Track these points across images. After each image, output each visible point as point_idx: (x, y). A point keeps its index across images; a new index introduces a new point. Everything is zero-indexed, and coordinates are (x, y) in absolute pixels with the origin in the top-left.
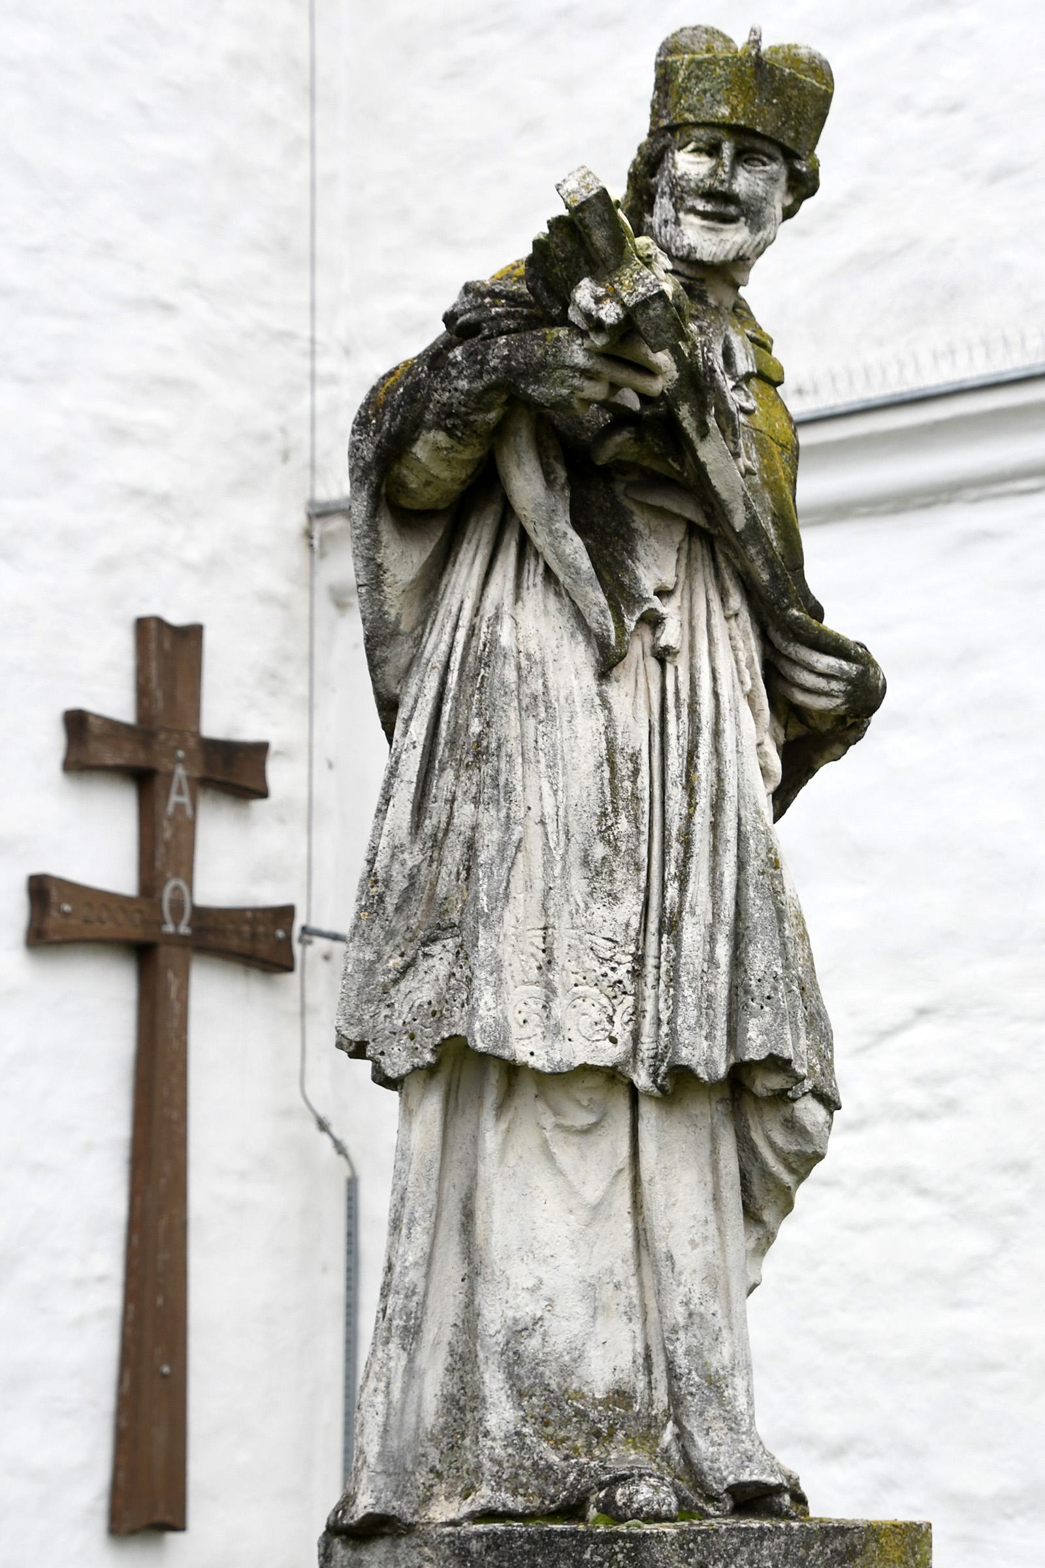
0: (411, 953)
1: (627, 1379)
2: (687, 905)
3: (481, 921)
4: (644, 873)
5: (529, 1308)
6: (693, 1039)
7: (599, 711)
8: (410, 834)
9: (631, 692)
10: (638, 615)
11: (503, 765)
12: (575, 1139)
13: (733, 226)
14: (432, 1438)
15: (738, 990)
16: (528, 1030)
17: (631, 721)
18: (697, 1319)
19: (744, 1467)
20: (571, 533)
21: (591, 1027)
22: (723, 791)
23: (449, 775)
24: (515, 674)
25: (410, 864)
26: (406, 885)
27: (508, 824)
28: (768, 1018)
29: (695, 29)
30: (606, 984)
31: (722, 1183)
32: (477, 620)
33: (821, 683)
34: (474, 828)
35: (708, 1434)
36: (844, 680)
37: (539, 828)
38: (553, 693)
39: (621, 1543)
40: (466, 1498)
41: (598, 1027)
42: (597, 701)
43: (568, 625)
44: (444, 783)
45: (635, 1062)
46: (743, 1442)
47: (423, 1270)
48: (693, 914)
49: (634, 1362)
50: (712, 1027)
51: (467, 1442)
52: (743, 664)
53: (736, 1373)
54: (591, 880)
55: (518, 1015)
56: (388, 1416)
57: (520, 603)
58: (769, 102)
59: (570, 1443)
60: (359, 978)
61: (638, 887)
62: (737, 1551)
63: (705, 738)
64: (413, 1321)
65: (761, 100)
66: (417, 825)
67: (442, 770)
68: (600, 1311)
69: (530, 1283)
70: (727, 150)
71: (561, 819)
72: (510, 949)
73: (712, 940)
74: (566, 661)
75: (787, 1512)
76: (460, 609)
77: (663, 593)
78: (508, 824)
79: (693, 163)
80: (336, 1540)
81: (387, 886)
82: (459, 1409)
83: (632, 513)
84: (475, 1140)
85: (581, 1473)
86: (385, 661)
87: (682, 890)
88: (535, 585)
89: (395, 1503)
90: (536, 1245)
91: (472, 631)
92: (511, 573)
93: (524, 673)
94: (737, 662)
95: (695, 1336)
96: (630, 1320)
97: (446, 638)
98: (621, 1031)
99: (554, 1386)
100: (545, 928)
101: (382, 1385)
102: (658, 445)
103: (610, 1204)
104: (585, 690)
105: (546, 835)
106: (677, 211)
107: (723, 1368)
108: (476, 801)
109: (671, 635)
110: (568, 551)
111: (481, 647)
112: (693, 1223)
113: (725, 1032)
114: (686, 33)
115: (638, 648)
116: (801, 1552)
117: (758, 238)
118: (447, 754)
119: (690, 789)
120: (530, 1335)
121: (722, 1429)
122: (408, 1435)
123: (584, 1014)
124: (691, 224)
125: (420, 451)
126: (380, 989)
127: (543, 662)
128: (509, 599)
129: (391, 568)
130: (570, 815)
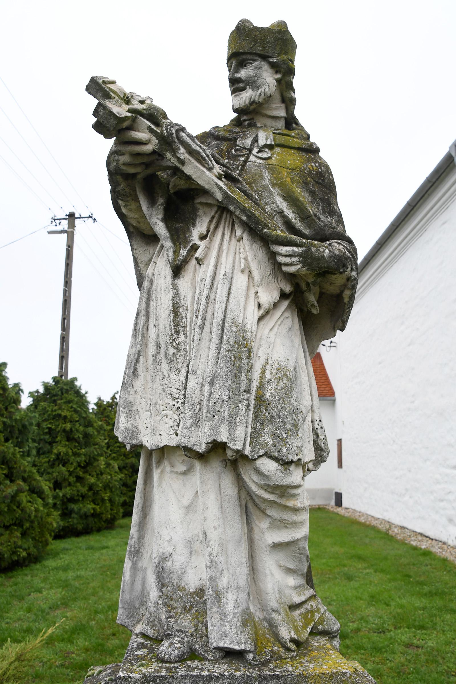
5: (168, 549)
6: (188, 434)
7: (171, 291)
10: (188, 248)
12: (181, 477)
19: (221, 639)
21: (169, 428)
30: (175, 409)
33: (287, 260)
36: (297, 256)
42: (171, 287)
46: (226, 626)
53: (229, 591)
58: (244, 40)
65: (241, 40)
68: (194, 553)
72: (139, 397)
83: (199, 209)
89: (126, 621)
99: (175, 584)
103: (196, 506)
110: (157, 229)
112: (214, 518)
121: (217, 618)
123: (166, 423)
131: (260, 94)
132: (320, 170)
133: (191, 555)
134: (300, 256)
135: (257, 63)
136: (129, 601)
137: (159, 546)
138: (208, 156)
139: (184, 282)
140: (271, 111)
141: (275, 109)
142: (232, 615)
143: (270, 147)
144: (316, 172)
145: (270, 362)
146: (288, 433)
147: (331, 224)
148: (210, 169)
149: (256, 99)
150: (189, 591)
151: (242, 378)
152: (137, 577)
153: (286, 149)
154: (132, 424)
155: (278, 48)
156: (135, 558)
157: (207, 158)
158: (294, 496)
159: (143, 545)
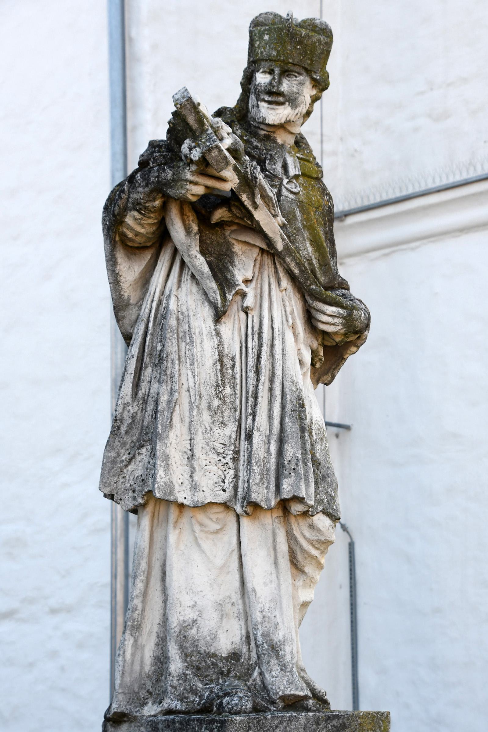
0: (133, 453)
1: (238, 648)
2: (255, 427)
3: (158, 437)
4: (238, 413)
5: (190, 615)
6: (258, 490)
7: (214, 337)
8: (132, 397)
9: (231, 328)
10: (234, 292)
11: (169, 365)
12: (211, 536)
13: (283, 107)
14: (149, 676)
15: (280, 466)
16: (183, 488)
17: (231, 342)
18: (267, 619)
20: (199, 256)
21: (213, 485)
22: (274, 373)
23: (149, 370)
24: (175, 322)
25: (132, 412)
26: (130, 421)
27: (172, 392)
28: (293, 479)
29: (266, 14)
30: (221, 464)
31: (278, 555)
32: (162, 297)
33: (330, 319)
34: (158, 394)
35: (271, 672)
36: (341, 318)
37: (187, 393)
38: (192, 330)
39: (216, 724)
40: (160, 704)
41: (217, 485)
42: (214, 333)
43: (201, 298)
44: (148, 372)
45: (236, 500)
47: (141, 599)
48: (259, 431)
49: (241, 639)
50: (269, 483)
51: (163, 678)
52: (288, 313)
53: (286, 644)
54: (212, 416)
55: (179, 481)
56: (124, 666)
57: (180, 289)
59: (209, 678)
60: (109, 465)
61: (235, 419)
62: (277, 727)
63: (265, 349)
64: (136, 623)
66: (135, 394)
67: (146, 367)
68: (225, 616)
69: (191, 603)
70: (277, 71)
71: (197, 389)
72: (174, 450)
73: (269, 443)
74: (199, 315)
75: (311, 708)
76: (155, 292)
77: (247, 282)
78: (172, 392)
79: (262, 78)
80: (108, 724)
81: (121, 422)
82: (161, 663)
84: (166, 538)
85: (211, 692)
86: (123, 317)
87: (254, 420)
88: (187, 280)
90: (193, 586)
91: (160, 302)
92: (176, 276)
93: (180, 321)
94: (286, 312)
95: (266, 627)
96: (239, 620)
97: (148, 306)
98: (228, 486)
100: (191, 440)
101: (121, 652)
102: (239, 213)
103: (229, 566)
104: (208, 328)
105: (190, 396)
106: (257, 101)
107: (280, 641)
108: (159, 382)
109: (249, 301)
110: (197, 264)
111: (163, 310)
113: (274, 485)
114: (262, 16)
115: (234, 308)
116: (314, 726)
118: (148, 360)
119: (258, 372)
120: (191, 628)
121: (278, 670)
122: (136, 675)
123: (210, 479)
124: (263, 107)
125: (129, 220)
126: (119, 470)
127: (189, 316)
128: (175, 287)
129: (123, 275)
130: (201, 387)
133: (221, 619)
134: (344, 318)
135: (302, 78)
136: (129, 685)
137: (178, 614)
139: (227, 329)
142: (291, 666)
150: (221, 656)
151: (306, 438)
152: (137, 656)
154: (169, 479)
156: (137, 634)
159: (144, 619)
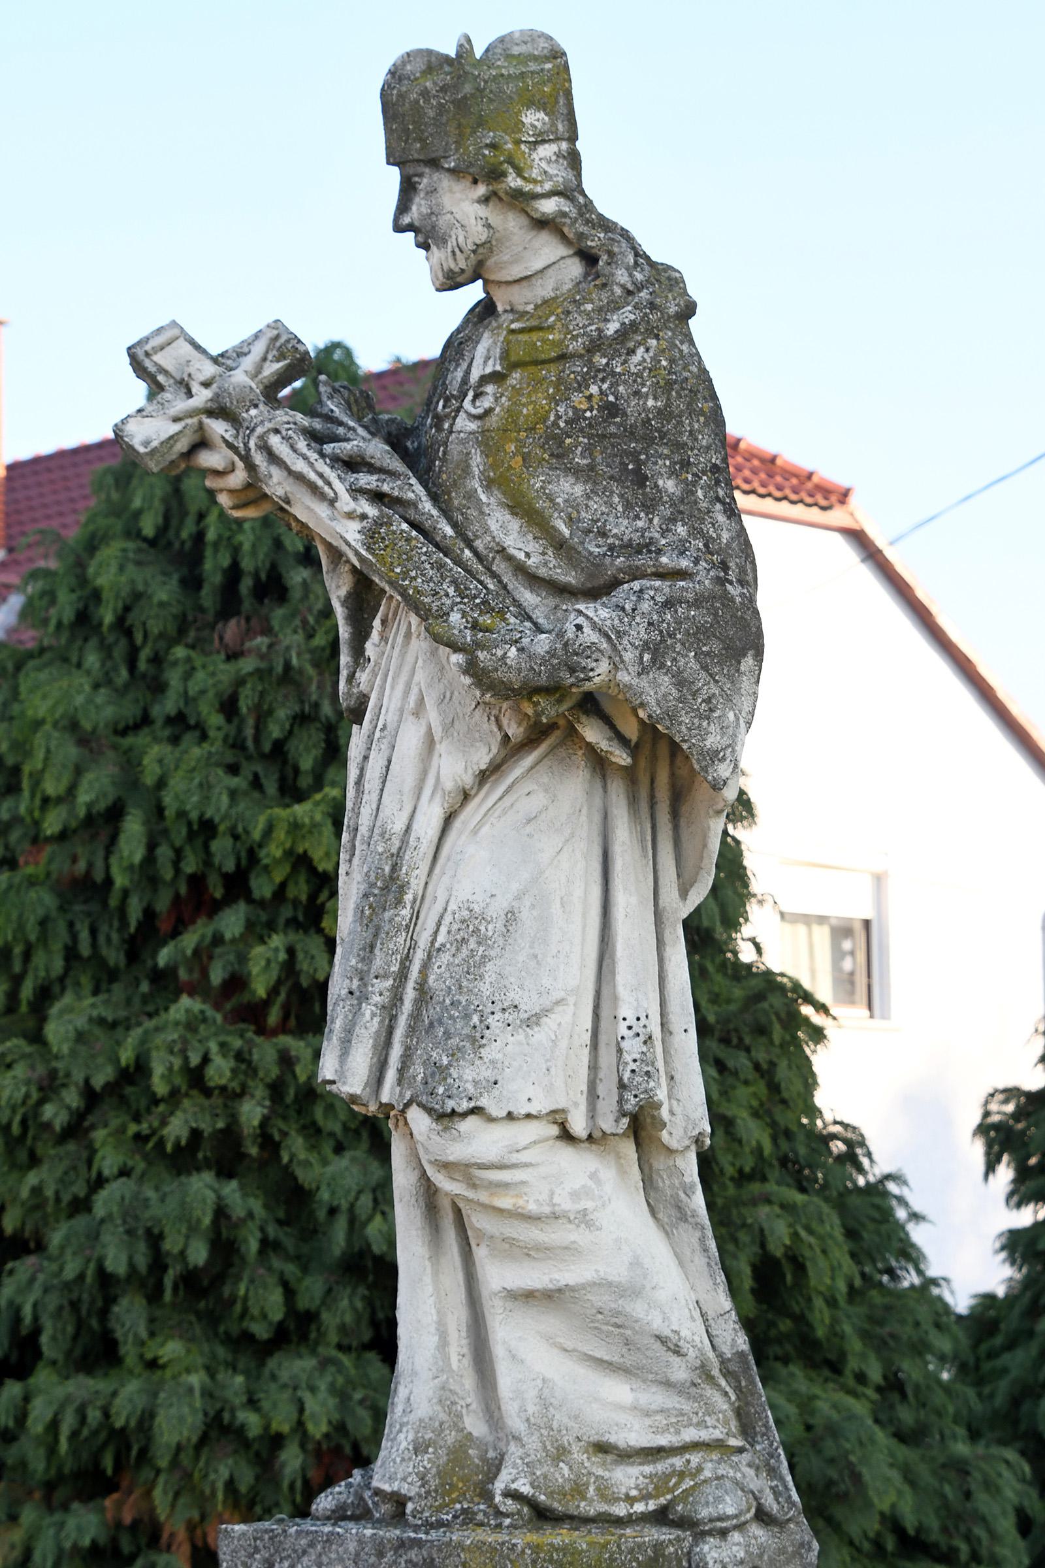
62: (304, 1552)
116: (373, 1559)
117: (449, 250)
131: (453, 252)
132: (611, 398)
135: (425, 181)
138: (321, 475)
140: (504, 272)
141: (511, 263)
143: (496, 378)
144: (600, 408)
145: (452, 907)
146: (453, 1055)
147: (643, 536)
148: (332, 502)
149: (453, 266)
153: (532, 369)
155: (452, 129)
157: (320, 483)
158: (506, 1186)
